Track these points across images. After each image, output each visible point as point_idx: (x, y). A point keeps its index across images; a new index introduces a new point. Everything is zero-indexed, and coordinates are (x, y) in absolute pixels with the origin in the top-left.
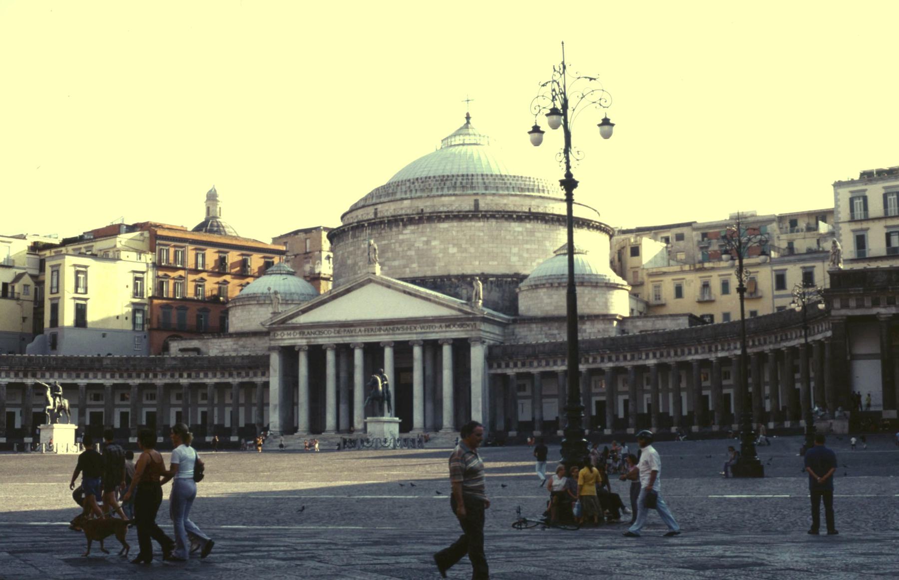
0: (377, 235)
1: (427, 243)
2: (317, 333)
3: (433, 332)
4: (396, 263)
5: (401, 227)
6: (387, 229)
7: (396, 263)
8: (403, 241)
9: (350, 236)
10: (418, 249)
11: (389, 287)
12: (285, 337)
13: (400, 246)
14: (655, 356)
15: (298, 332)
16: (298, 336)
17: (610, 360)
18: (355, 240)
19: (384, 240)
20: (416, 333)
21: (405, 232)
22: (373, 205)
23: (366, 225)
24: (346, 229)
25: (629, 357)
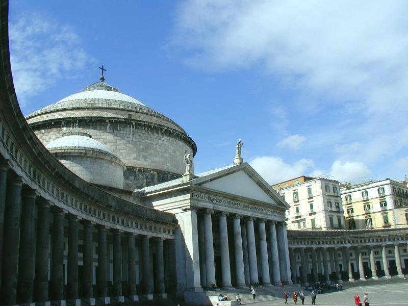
0: (141, 134)
1: (174, 151)
2: (218, 200)
3: (270, 215)
4: (157, 159)
5: (160, 135)
6: (150, 133)
7: (157, 159)
8: (161, 145)
9: (108, 127)
10: (170, 154)
11: (250, 177)
12: (199, 198)
13: (160, 148)
14: (349, 242)
15: (207, 196)
16: (207, 200)
17: (327, 243)
18: (115, 131)
19: (148, 140)
20: (264, 214)
21: (162, 139)
22: (128, 111)
23: (134, 124)
24: (107, 121)
25: (336, 242)
